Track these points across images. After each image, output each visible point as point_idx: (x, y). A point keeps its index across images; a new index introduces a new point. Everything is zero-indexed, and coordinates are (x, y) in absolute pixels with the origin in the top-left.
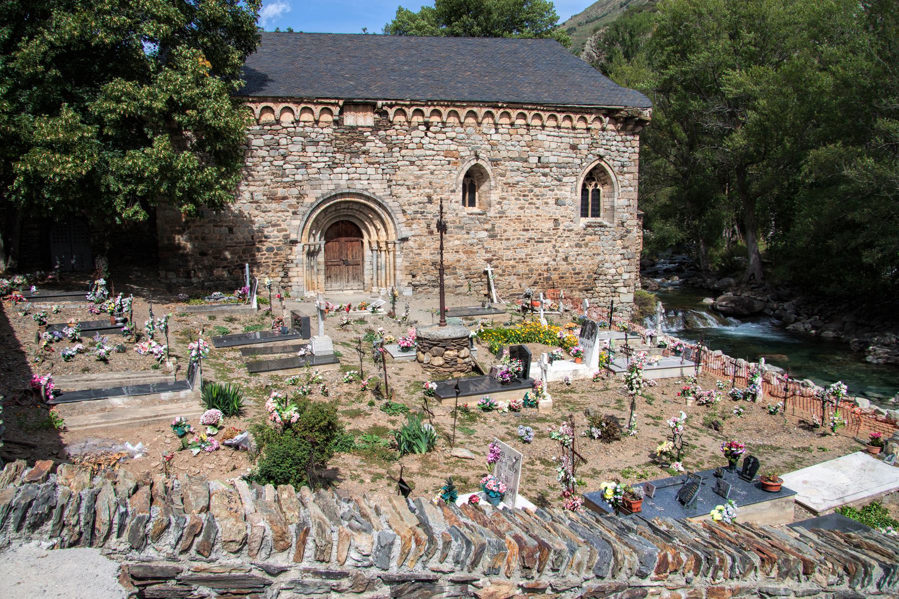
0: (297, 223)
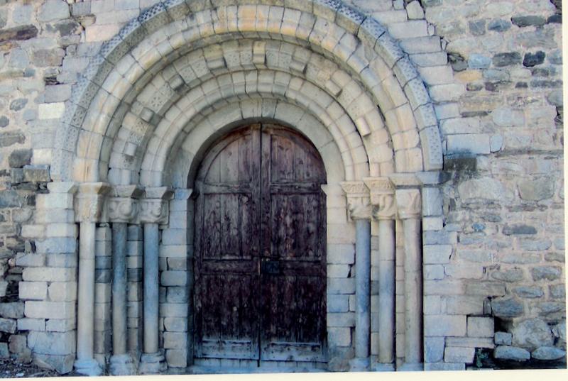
0: (54, 111)
